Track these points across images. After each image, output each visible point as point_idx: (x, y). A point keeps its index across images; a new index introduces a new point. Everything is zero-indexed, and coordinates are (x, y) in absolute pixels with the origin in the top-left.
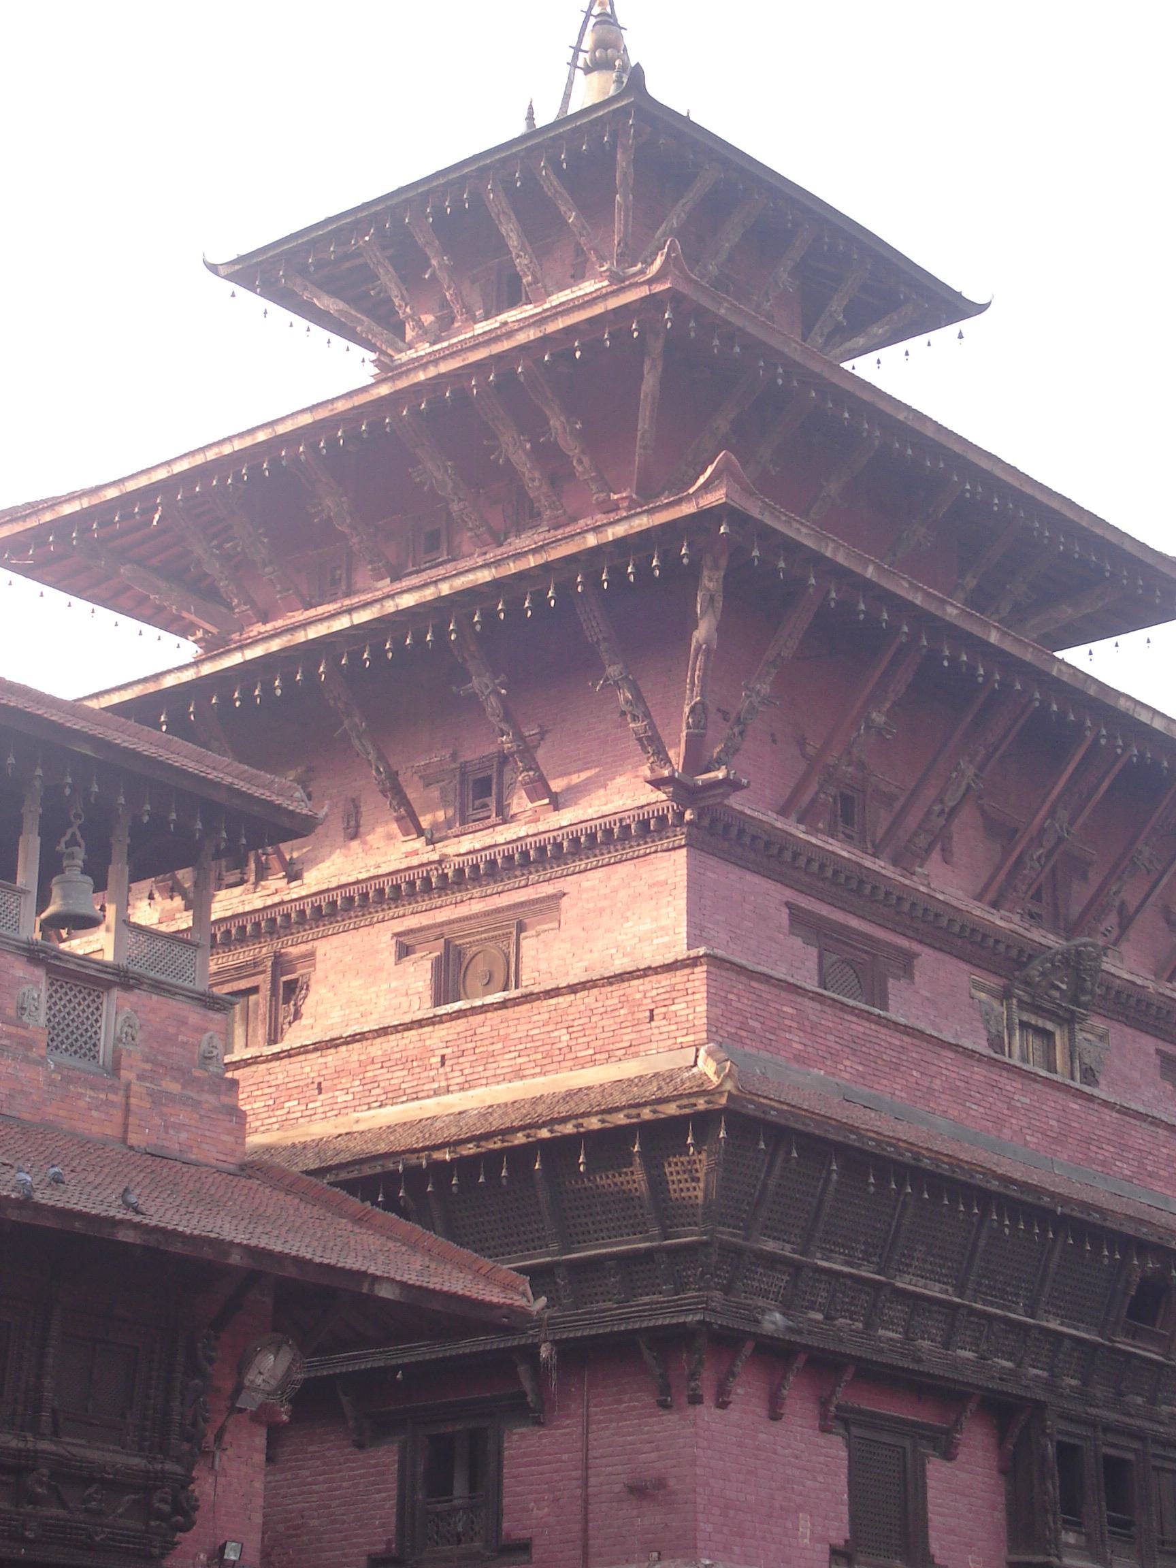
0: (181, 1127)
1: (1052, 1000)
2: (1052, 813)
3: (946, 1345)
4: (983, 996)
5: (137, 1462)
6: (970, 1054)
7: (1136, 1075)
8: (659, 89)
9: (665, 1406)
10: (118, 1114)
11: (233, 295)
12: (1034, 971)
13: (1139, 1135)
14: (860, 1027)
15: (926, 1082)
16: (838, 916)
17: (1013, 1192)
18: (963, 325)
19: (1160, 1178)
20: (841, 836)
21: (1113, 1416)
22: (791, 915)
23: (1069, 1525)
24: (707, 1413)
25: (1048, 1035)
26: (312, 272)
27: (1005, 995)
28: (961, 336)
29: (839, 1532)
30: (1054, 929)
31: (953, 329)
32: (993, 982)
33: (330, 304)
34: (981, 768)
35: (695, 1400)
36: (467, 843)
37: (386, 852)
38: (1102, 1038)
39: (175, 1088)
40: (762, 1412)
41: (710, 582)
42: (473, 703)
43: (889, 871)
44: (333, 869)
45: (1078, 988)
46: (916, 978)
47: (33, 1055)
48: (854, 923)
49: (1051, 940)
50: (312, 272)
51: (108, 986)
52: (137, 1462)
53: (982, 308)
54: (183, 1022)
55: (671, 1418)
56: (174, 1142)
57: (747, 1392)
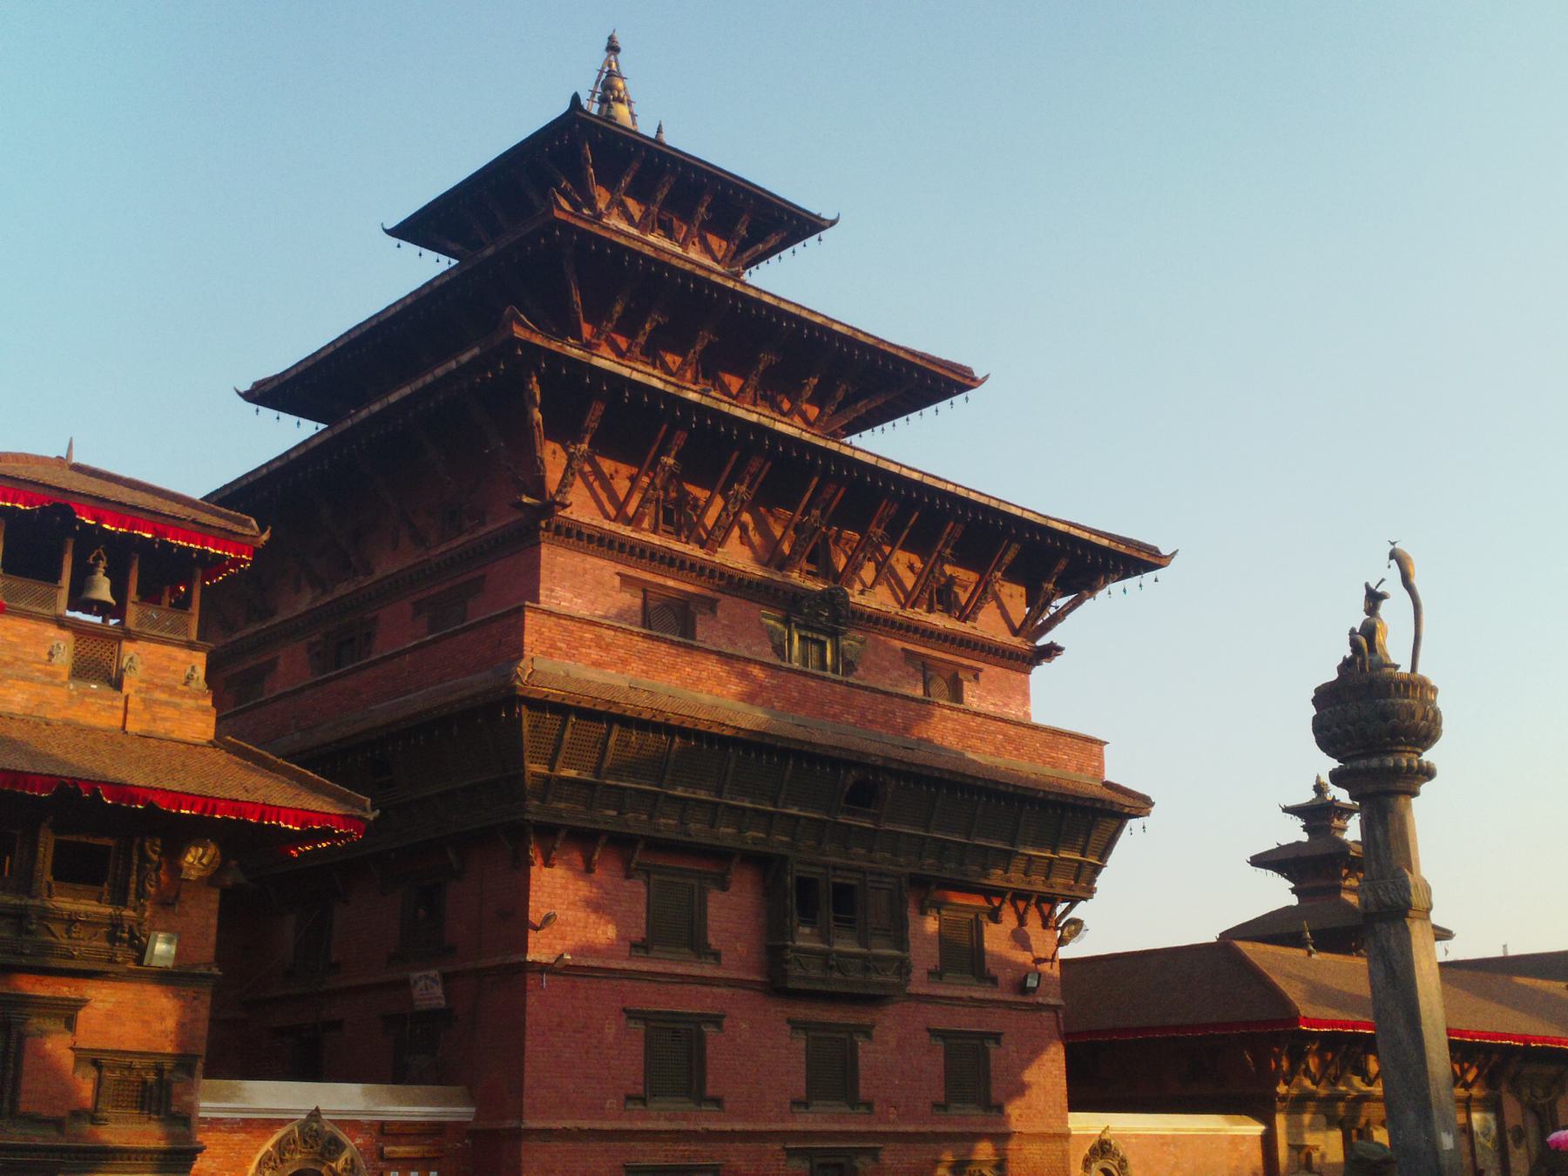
0: (164, 719)
2: (806, 512)
3: (712, 826)
10: (120, 714)
16: (660, 580)
23: (804, 923)
25: (822, 645)
27: (786, 622)
38: (861, 643)
43: (699, 553)
45: (836, 617)
47: (57, 681)
48: (671, 583)
56: (160, 728)
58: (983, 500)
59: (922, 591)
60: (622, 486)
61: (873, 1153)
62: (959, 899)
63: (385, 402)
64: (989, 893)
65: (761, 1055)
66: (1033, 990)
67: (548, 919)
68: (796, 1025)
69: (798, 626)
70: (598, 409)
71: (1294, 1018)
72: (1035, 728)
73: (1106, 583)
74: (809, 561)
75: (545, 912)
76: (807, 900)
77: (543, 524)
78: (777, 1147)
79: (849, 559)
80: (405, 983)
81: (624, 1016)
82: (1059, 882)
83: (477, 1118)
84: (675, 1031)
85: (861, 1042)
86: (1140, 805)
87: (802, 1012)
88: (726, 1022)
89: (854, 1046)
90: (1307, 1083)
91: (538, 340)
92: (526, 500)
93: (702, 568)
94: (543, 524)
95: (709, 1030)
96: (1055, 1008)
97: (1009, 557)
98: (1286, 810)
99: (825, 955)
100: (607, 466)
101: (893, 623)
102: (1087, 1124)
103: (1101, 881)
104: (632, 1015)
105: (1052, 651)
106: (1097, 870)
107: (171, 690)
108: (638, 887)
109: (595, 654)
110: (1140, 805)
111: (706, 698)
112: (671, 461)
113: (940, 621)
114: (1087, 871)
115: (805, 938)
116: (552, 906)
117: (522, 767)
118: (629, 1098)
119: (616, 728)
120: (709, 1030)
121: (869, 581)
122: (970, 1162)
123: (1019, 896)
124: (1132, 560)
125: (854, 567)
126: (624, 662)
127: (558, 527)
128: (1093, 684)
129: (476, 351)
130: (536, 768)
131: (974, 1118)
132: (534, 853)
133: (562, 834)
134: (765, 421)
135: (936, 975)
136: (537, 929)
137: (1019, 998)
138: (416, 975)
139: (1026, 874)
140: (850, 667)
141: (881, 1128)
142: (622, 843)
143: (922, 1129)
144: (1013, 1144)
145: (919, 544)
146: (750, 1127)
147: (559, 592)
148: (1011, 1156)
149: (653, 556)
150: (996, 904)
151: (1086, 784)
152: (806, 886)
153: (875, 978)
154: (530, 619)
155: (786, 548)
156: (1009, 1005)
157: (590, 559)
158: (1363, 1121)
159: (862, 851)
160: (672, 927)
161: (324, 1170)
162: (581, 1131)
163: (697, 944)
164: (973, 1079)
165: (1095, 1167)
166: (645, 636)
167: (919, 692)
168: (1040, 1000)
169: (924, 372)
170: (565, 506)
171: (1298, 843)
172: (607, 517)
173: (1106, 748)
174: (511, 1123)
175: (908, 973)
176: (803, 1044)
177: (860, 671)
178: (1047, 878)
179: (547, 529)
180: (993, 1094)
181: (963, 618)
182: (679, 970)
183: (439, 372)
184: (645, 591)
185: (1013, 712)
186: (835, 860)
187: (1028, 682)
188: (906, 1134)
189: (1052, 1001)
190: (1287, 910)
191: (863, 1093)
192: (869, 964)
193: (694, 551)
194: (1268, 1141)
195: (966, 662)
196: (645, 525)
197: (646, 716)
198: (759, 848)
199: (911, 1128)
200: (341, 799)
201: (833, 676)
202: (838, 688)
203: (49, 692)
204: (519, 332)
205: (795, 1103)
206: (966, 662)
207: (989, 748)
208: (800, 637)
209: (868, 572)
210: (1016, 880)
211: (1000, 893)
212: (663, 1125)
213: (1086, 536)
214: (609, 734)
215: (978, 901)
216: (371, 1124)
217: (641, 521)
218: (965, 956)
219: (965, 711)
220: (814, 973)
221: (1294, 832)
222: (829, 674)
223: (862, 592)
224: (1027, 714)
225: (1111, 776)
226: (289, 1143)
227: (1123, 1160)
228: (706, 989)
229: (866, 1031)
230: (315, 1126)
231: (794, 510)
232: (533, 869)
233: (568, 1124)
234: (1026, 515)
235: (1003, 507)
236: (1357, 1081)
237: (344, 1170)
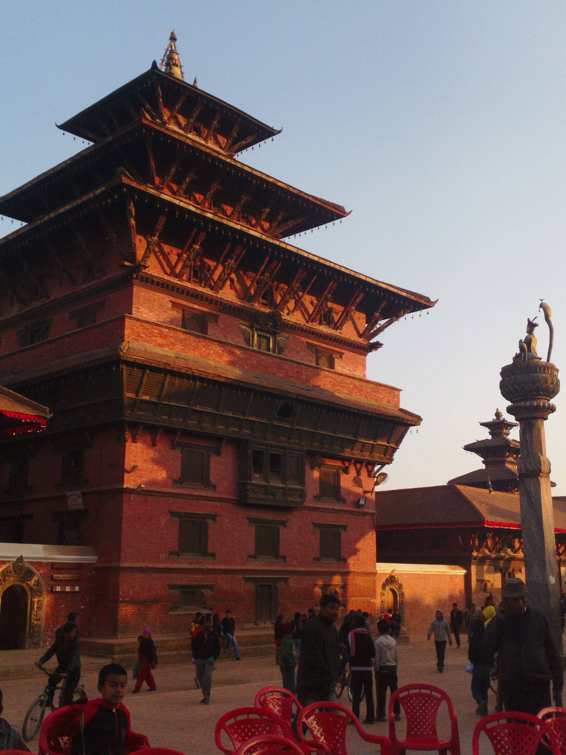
1: (268, 328)
2: (263, 274)
3: (214, 425)
4: (244, 327)
7: (299, 349)
11: (64, 134)
15: (208, 351)
16: (191, 305)
18: (274, 137)
19: (294, 377)
20: (192, 282)
21: (273, 443)
22: (172, 305)
23: (256, 472)
25: (269, 338)
26: (74, 126)
27: (251, 327)
28: (273, 140)
29: (177, 475)
30: (270, 307)
31: (271, 138)
34: (236, 261)
38: (287, 338)
43: (211, 293)
46: (219, 323)
48: (196, 307)
50: (74, 126)
53: (279, 132)
58: (347, 271)
59: (316, 314)
60: (173, 259)
61: (286, 580)
62: (329, 462)
63: (57, 213)
64: (343, 460)
65: (233, 534)
66: (363, 506)
67: (134, 468)
69: (257, 329)
70: (162, 220)
71: (482, 521)
72: (368, 382)
73: (404, 314)
74: (264, 298)
75: (133, 464)
76: (258, 461)
77: (135, 276)
78: (241, 577)
79: (282, 298)
80: (64, 497)
81: (170, 514)
82: (377, 455)
85: (281, 528)
86: (416, 420)
87: (254, 514)
88: (218, 518)
89: (278, 530)
90: (487, 551)
91: (134, 185)
92: (126, 263)
93: (212, 300)
94: (135, 276)
95: (210, 521)
96: (372, 514)
97: (358, 300)
98: (482, 424)
99: (266, 488)
100: (167, 248)
101: (303, 329)
102: (385, 568)
103: (396, 456)
104: (173, 514)
105: (377, 345)
106: (394, 450)
108: (177, 453)
109: (159, 340)
110: (416, 420)
111: (212, 363)
112: (198, 247)
113: (324, 329)
114: (390, 451)
115: (257, 479)
116: (135, 461)
117: (123, 394)
118: (172, 553)
119: (168, 376)
120: (210, 521)
121: (291, 309)
122: (329, 585)
123: (358, 462)
125: (285, 302)
126: (173, 344)
127: (142, 278)
128: (396, 361)
129: (103, 188)
130: (129, 395)
131: (333, 565)
132: (128, 435)
133: (142, 427)
134: (244, 229)
135: (317, 498)
136: (129, 472)
137: (356, 510)
138: (69, 493)
139: (361, 451)
140: (281, 350)
141: (290, 569)
142: (170, 432)
143: (309, 569)
144: (350, 577)
145: (316, 292)
147: (142, 309)
148: (349, 582)
149: (188, 294)
150: (347, 464)
151: (391, 409)
152: (258, 455)
153: (290, 499)
154: (128, 322)
155: (252, 292)
156: (351, 512)
157: (157, 294)
158: (511, 569)
159: (285, 439)
160: (194, 473)
161: (24, 585)
162: (148, 568)
163: (206, 483)
164: (334, 546)
165: (387, 588)
166: (183, 332)
167: (314, 364)
168: (366, 510)
169: (320, 207)
170: (145, 267)
171: (487, 440)
172: (166, 273)
173: (401, 392)
174: (114, 564)
175: (305, 496)
176: (253, 529)
177: (286, 352)
178: (371, 453)
179: (136, 279)
180: (342, 554)
181: (336, 328)
182: (197, 493)
183: (85, 198)
184: (183, 310)
185: (358, 374)
186: (271, 442)
187: (365, 360)
188: (301, 571)
189: (371, 511)
190: (480, 471)
192: (285, 492)
193: (207, 291)
194: (467, 578)
195: (336, 349)
196: (184, 278)
197: (183, 371)
198: (234, 436)
199: (303, 569)
200: (34, 408)
201: (273, 354)
202: (275, 360)
204: (125, 180)
205: (249, 556)
206: (336, 349)
207: (346, 391)
208: (258, 335)
209: (291, 305)
210: (357, 454)
211: (349, 460)
212: (187, 566)
213: (396, 291)
214: (165, 380)
215: (339, 464)
216: (48, 564)
217: (183, 276)
218: (331, 489)
219: (335, 373)
220: (261, 496)
221: (485, 435)
222: (271, 353)
223: (288, 314)
224: (365, 375)
225: (403, 406)
226: (7, 572)
227: (401, 586)
228: (209, 503)
229: (284, 524)
230: (20, 564)
231: (257, 273)
232: (128, 444)
233: (143, 565)
234: (368, 280)
235: (357, 275)
236: (509, 551)
237: (34, 585)
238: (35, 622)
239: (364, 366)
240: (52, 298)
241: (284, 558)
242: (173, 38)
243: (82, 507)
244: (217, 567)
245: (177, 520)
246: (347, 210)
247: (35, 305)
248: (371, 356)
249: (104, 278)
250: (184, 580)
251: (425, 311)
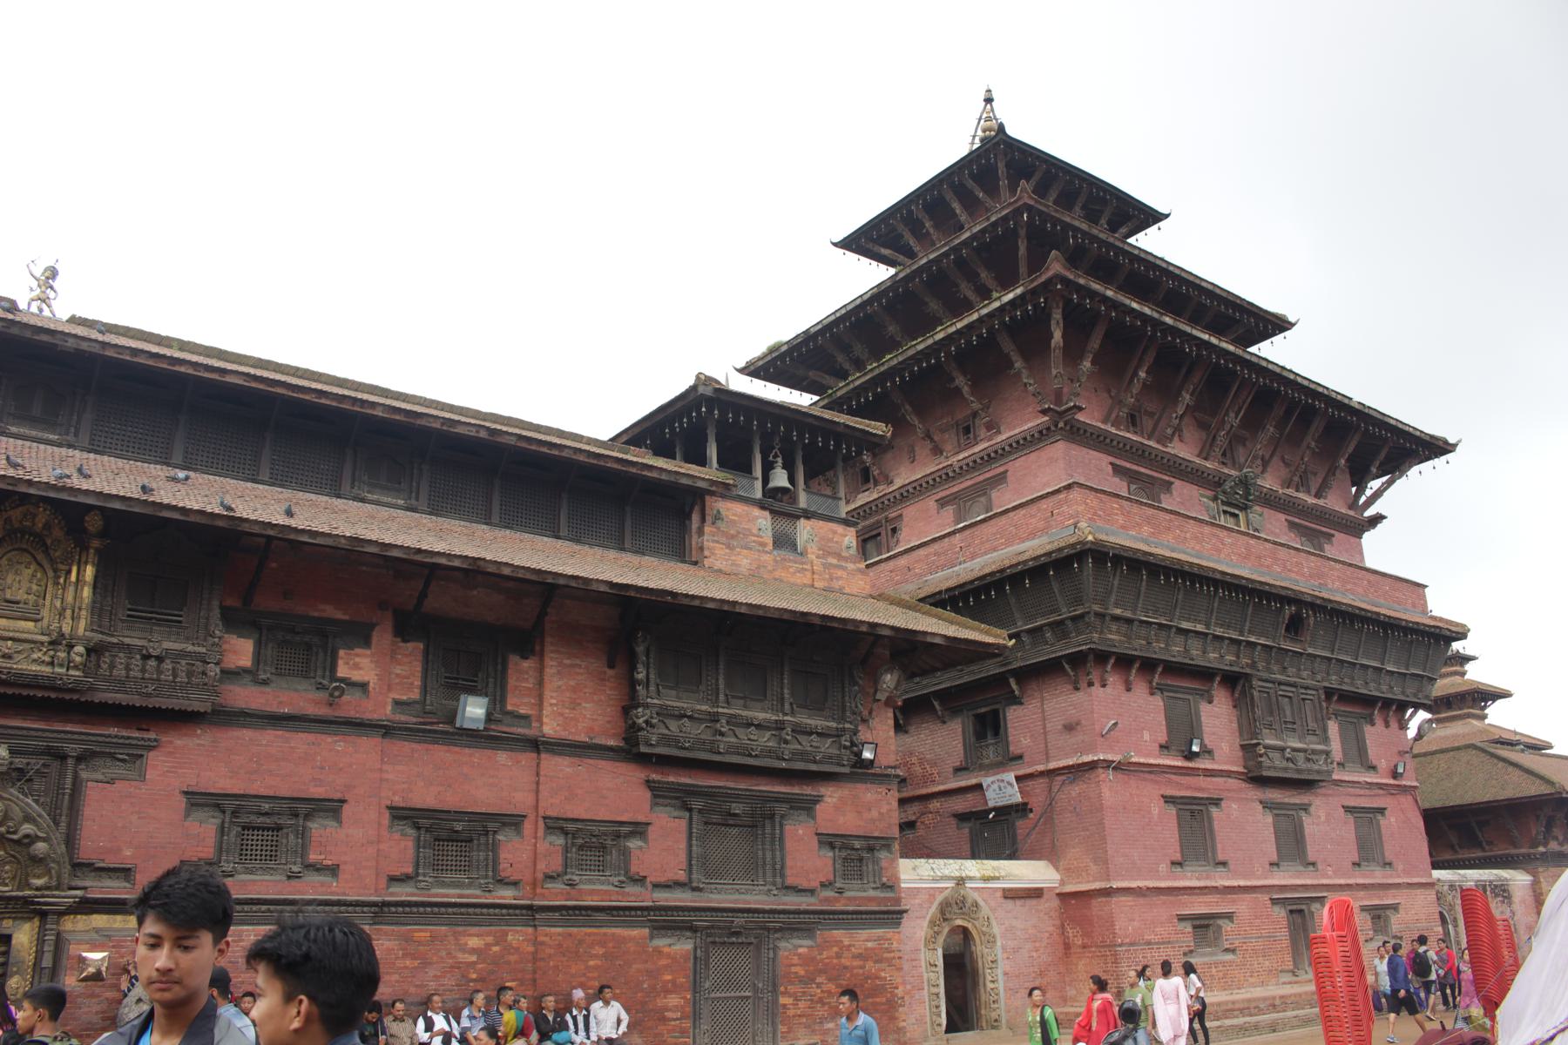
0: (838, 579)
5: (834, 725)
6: (1201, 521)
8: (1012, 131)
9: (1077, 689)
10: (809, 574)
12: (1227, 486)
13: (1282, 552)
14: (1151, 511)
16: (1135, 467)
17: (1228, 579)
18: (1161, 224)
24: (1097, 690)
25: (1236, 516)
27: (1215, 499)
29: (1162, 737)
32: (1210, 493)
33: (886, 252)
35: (1090, 684)
36: (961, 456)
37: (926, 467)
39: (835, 561)
40: (1121, 687)
41: (1057, 315)
42: (958, 390)
44: (904, 476)
48: (1143, 470)
49: (1233, 473)
51: (798, 517)
52: (834, 725)
53: (1167, 216)
54: (835, 532)
55: (1080, 694)
57: (1113, 679)
68: (1266, 805)
83: (1062, 882)
84: (1192, 812)
95: (1213, 810)
99: (1282, 749)
104: (1169, 800)
105: (1377, 519)
107: (839, 556)
108: (1158, 702)
118: (1173, 863)
124: (1435, 448)
130: (1096, 608)
133: (1112, 661)
137: (1392, 782)
142: (1149, 666)
146: (1249, 883)
176: (1270, 819)
191: (1311, 857)
192: (1310, 756)
199: (1342, 881)
203: (766, 557)
238: (991, 985)
239: (1361, 553)
240: (898, 483)
241: (1313, 864)
242: (989, 100)
243: (1018, 798)
244: (1235, 883)
245: (1172, 810)
246: (1292, 320)
247: (863, 499)
248: (1369, 539)
249: (1004, 437)
250: (1200, 906)
251: (1443, 458)
